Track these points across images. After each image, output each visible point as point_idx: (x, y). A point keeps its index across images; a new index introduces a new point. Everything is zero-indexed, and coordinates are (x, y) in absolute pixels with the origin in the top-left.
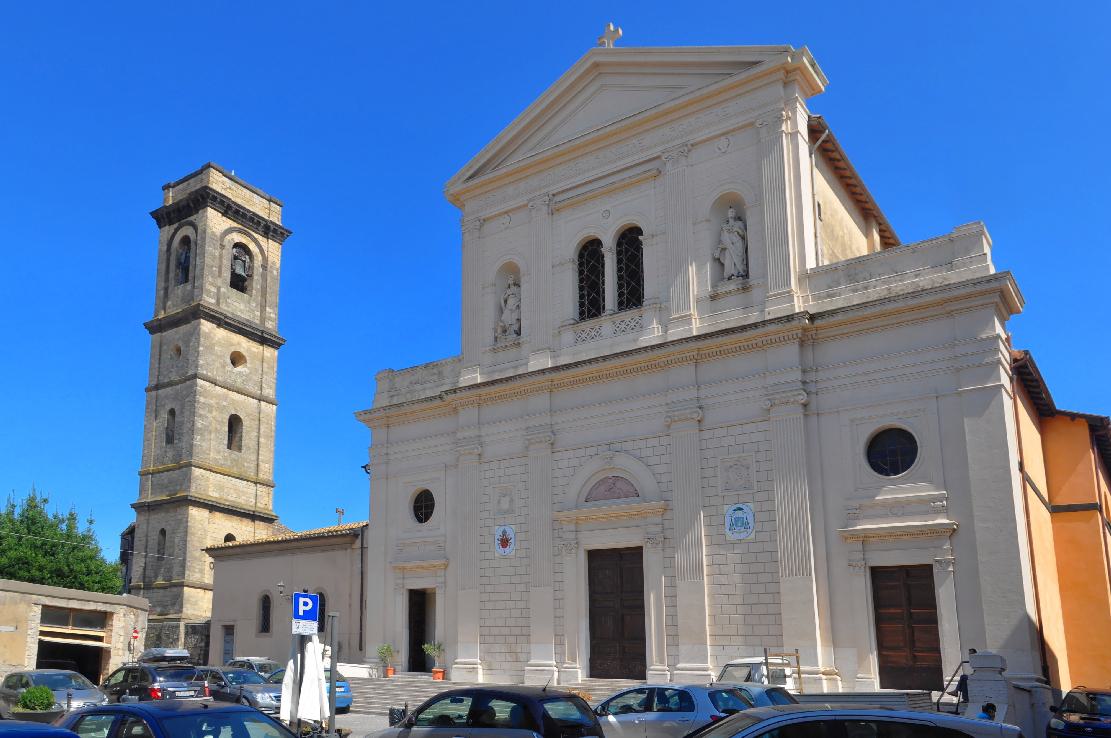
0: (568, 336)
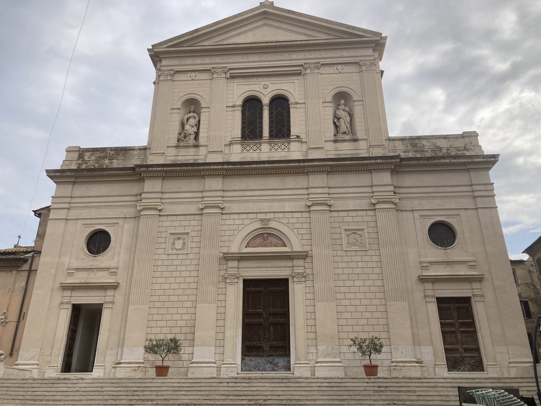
0: (237, 148)
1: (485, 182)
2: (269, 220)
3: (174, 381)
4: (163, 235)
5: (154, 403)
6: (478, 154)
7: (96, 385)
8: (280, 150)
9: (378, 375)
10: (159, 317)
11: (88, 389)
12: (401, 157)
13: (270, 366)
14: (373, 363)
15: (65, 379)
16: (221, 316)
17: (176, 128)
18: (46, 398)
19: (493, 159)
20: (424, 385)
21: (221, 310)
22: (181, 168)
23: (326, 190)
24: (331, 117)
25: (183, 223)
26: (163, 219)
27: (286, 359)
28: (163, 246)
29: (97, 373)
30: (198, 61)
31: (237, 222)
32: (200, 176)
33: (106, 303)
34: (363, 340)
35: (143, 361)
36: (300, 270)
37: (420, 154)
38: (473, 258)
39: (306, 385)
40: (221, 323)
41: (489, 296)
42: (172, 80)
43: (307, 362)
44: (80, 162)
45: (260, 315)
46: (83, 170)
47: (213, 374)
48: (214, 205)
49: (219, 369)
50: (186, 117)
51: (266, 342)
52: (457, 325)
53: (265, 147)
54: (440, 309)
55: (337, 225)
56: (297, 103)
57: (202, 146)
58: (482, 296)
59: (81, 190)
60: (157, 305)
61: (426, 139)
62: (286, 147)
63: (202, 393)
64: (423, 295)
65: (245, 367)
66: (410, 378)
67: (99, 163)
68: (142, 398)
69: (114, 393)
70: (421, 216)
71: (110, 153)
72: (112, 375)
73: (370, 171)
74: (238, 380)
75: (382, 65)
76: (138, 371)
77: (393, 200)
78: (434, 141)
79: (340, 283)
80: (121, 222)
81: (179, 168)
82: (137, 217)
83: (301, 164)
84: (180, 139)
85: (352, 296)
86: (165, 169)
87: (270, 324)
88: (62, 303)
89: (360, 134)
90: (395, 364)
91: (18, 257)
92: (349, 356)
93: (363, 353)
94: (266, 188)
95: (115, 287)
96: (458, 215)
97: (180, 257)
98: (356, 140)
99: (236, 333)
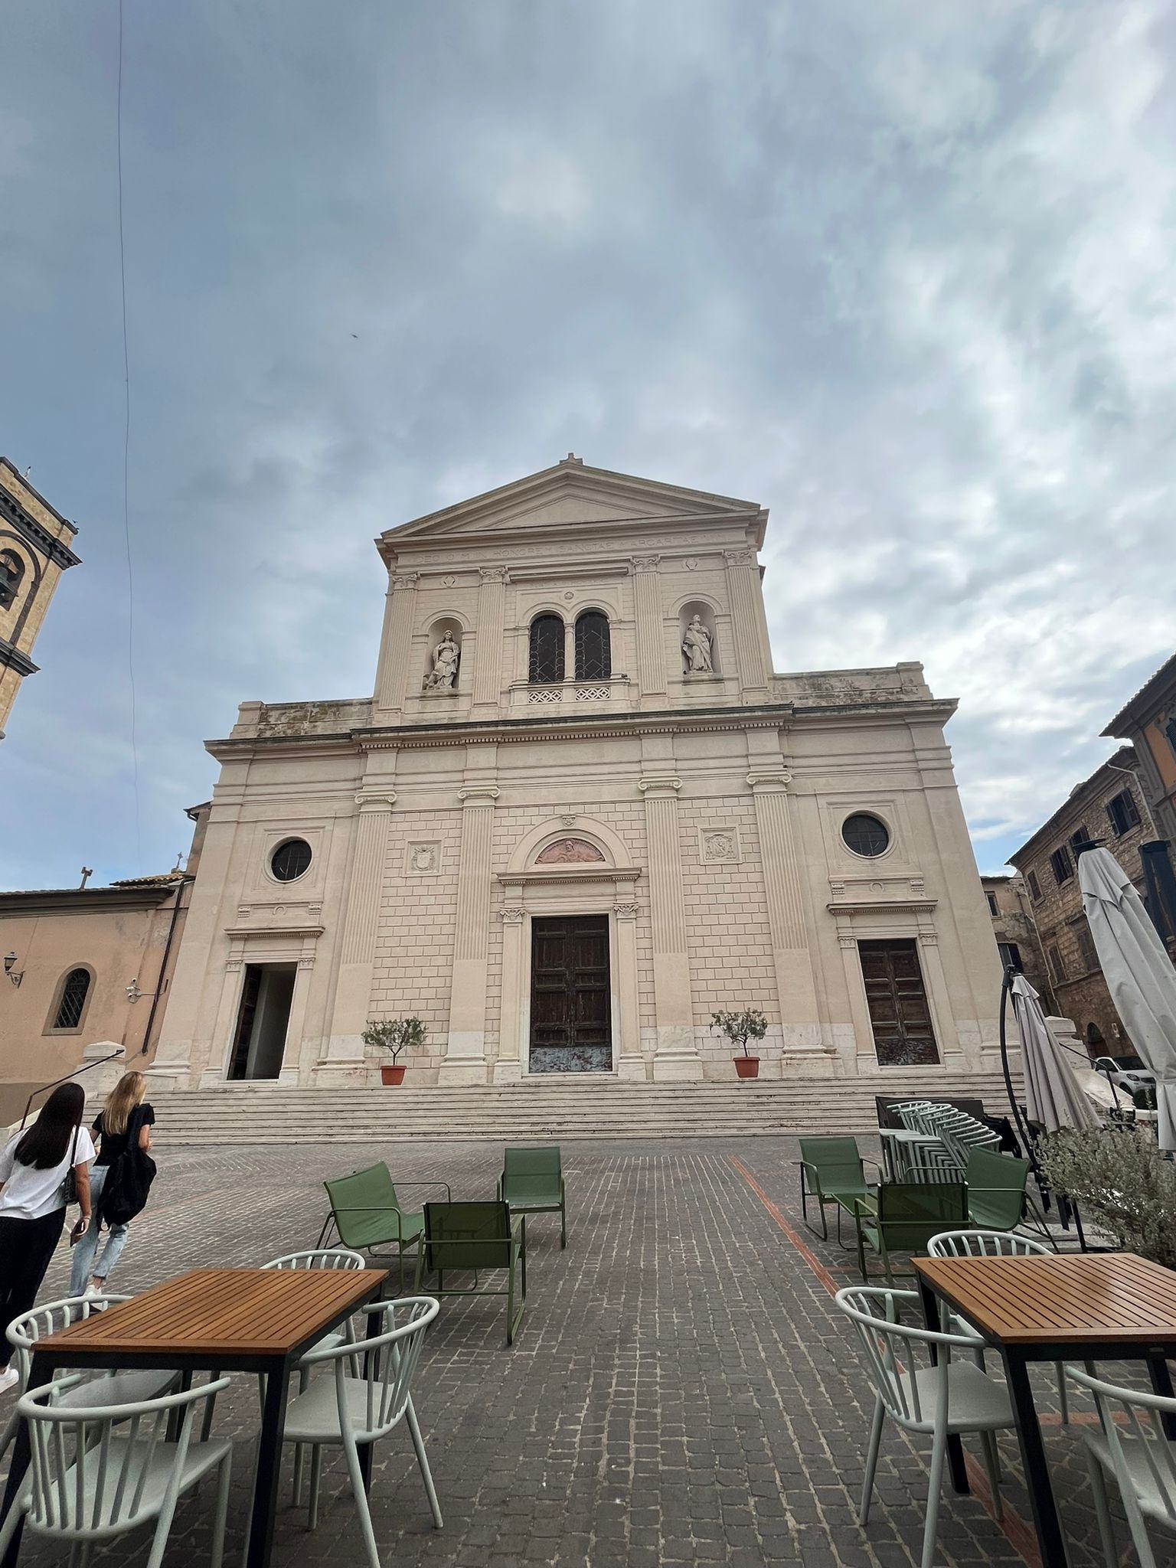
0: (521, 697)
1: (936, 745)
2: (574, 817)
3: (408, 1092)
4: (399, 845)
5: (369, 1131)
6: (923, 699)
7: (277, 1101)
9: (760, 1076)
10: (392, 983)
11: (261, 1109)
12: (795, 706)
13: (578, 1062)
14: (752, 1055)
15: (225, 1091)
16: (495, 980)
17: (420, 666)
18: (188, 1125)
19: (949, 707)
20: (836, 1090)
21: (495, 969)
22: (427, 732)
23: (671, 764)
24: (678, 643)
25: (431, 825)
26: (398, 818)
27: (604, 1050)
28: (397, 863)
29: (286, 1078)
30: (458, 557)
31: (521, 821)
32: (459, 744)
33: (302, 961)
34: (733, 1015)
35: (364, 1059)
36: (628, 900)
37: (827, 702)
38: (919, 873)
39: (632, 1095)
40: (494, 991)
41: (947, 937)
42: (414, 590)
43: (640, 1055)
44: (262, 727)
45: (560, 977)
46: (266, 740)
47: (480, 1078)
48: (482, 793)
49: (491, 1069)
50: (438, 648)
51: (570, 1022)
52: (894, 987)
53: (568, 694)
54: (864, 960)
55: (690, 823)
56: (621, 622)
57: (462, 695)
58: (935, 936)
59: (263, 773)
60: (388, 962)
61: (836, 676)
62: (604, 693)
63: (453, 1113)
64: (835, 936)
65: (536, 1066)
66: (811, 1080)
67: (294, 727)
68: (351, 1122)
69: (304, 1115)
70: (828, 804)
71: (312, 712)
72: (310, 1083)
73: (743, 731)
74: (518, 1090)
75: (762, 558)
76: (354, 1076)
77: (782, 778)
78: (849, 679)
79: (696, 920)
80: (328, 825)
81: (424, 733)
82: (354, 816)
83: (629, 721)
84: (427, 685)
85: (715, 941)
86: (401, 734)
87: (578, 992)
88: (229, 963)
89: (726, 669)
90: (789, 1056)
91: (157, 886)
92: (711, 1043)
93: (734, 1037)
94: (572, 762)
95: (317, 934)
96: (892, 801)
97: (426, 881)
98: (719, 681)
99: (520, 1006)
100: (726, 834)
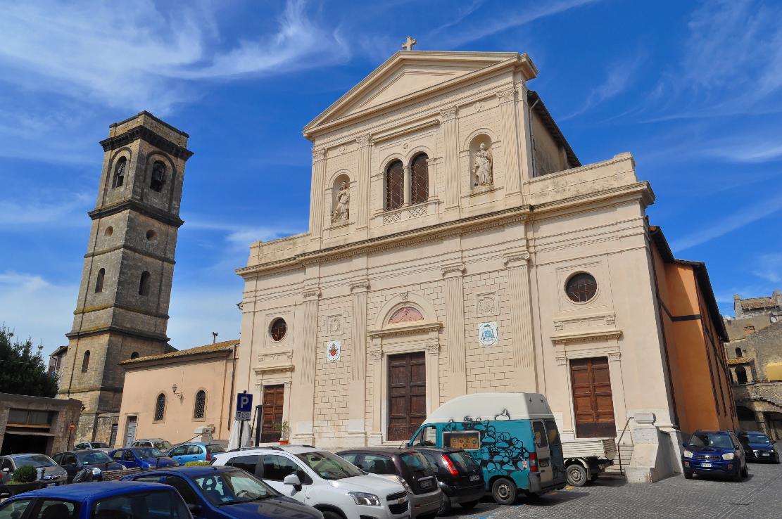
0: (381, 219)
8: (418, 216)
36: (435, 342)
53: (405, 215)
59: (264, 284)
80: (292, 309)
95: (292, 369)
98: (492, 191)
100: (491, 296)
